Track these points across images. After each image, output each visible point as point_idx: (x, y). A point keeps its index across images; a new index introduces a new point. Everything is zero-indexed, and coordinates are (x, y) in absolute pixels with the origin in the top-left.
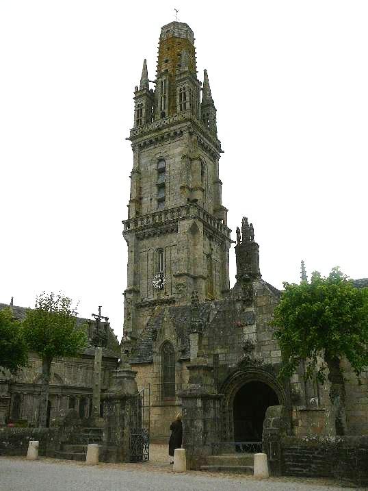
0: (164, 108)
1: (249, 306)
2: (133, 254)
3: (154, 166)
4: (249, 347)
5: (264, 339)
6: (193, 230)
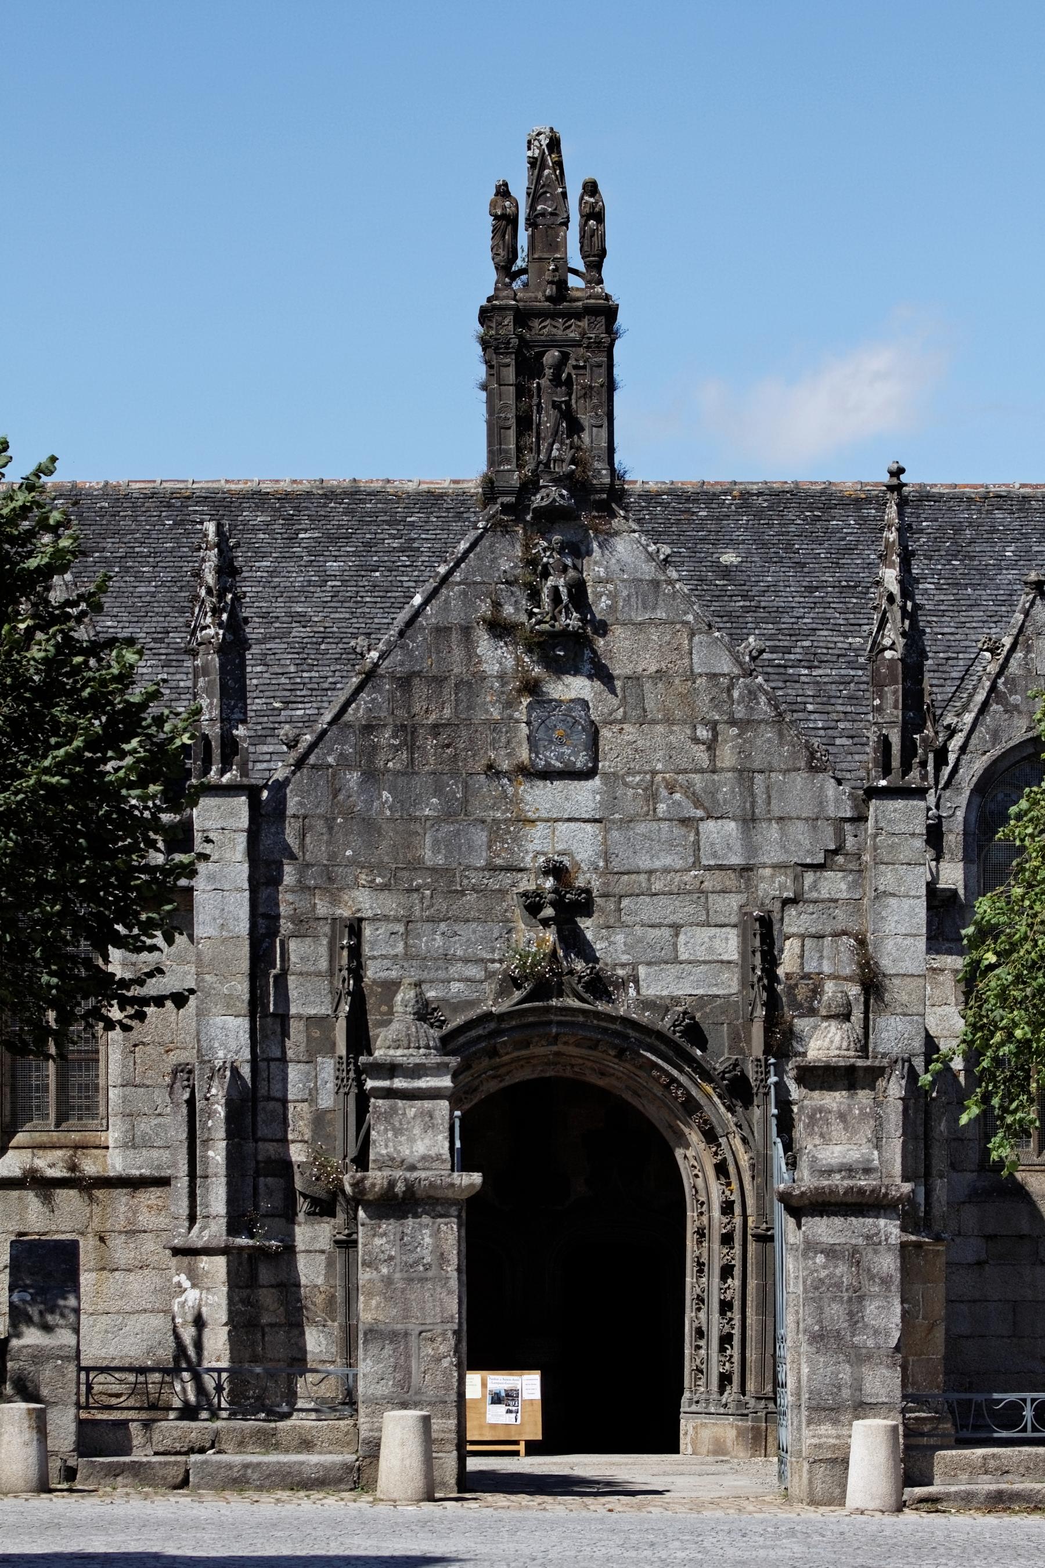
5: (644, 862)
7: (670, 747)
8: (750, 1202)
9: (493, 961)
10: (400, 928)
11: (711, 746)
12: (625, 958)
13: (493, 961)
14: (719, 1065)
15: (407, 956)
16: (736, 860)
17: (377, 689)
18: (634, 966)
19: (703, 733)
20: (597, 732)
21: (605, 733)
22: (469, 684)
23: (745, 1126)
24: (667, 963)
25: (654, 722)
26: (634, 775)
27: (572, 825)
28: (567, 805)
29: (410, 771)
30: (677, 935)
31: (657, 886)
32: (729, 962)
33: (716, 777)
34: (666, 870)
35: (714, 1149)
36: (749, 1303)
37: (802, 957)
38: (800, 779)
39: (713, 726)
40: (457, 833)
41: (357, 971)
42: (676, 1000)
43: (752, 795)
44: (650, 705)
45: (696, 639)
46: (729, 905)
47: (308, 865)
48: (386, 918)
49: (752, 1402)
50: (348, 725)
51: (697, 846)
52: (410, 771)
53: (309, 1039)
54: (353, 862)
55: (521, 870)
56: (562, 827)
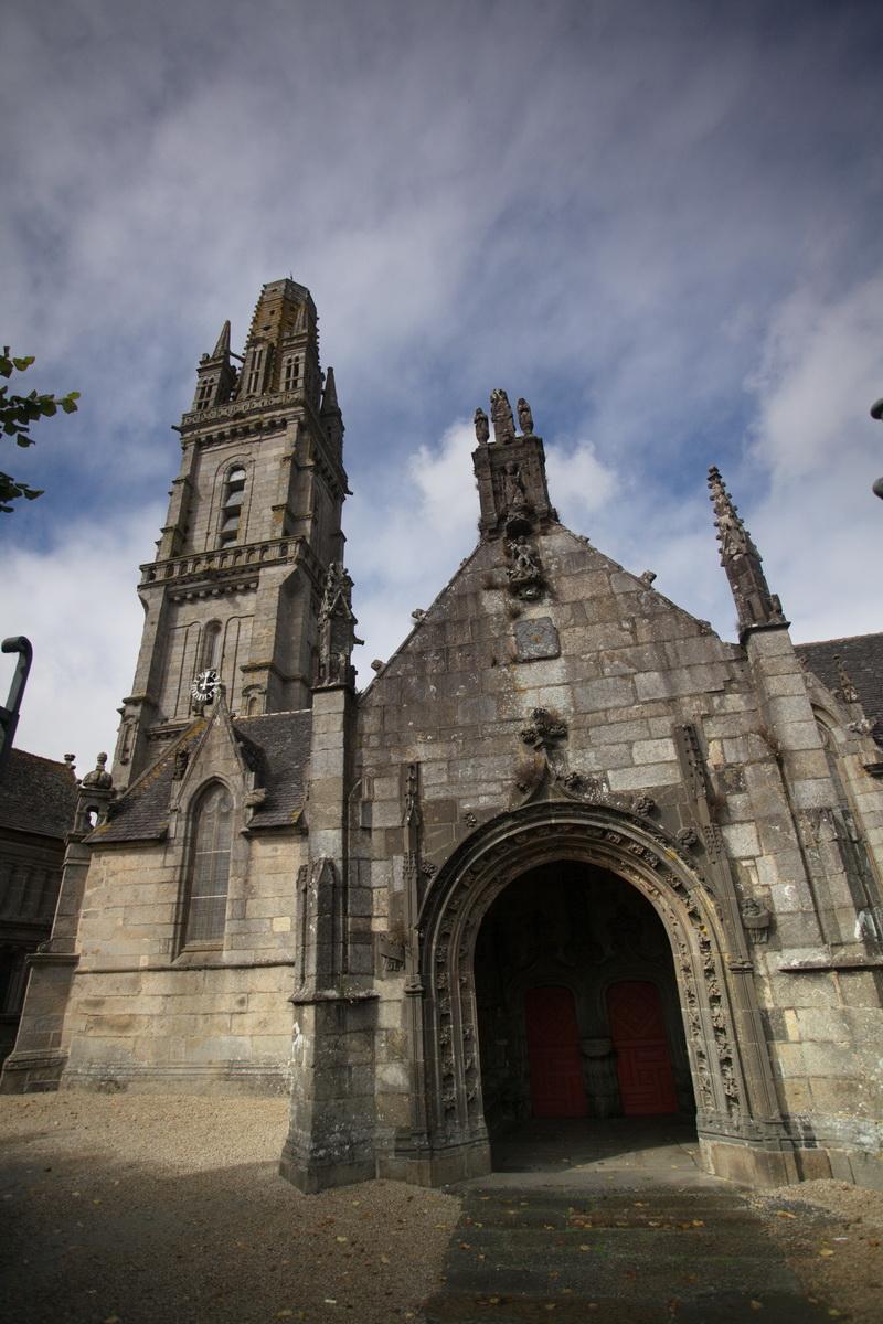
0: (255, 390)
1: (534, 600)
2: (155, 627)
3: (220, 478)
4: (548, 732)
5: (602, 705)
6: (289, 588)
7: (607, 636)
8: (723, 941)
9: (506, 780)
10: (444, 766)
11: (633, 632)
12: (597, 768)
13: (506, 780)
14: (681, 830)
15: (450, 783)
16: (662, 694)
17: (425, 632)
18: (604, 772)
19: (626, 625)
20: (558, 633)
21: (564, 634)
22: (479, 621)
23: (707, 879)
24: (627, 767)
25: (595, 623)
26: (586, 654)
27: (551, 689)
28: (545, 678)
29: (446, 672)
30: (631, 748)
31: (612, 718)
32: (671, 762)
33: (640, 648)
34: (617, 708)
35: (686, 901)
36: (739, 1030)
37: (723, 753)
38: (695, 642)
39: (632, 620)
40: (477, 704)
41: (416, 796)
42: (638, 792)
43: (666, 655)
44: (590, 614)
45: (612, 576)
46: (665, 724)
47: (386, 734)
48: (435, 760)
49: (763, 1128)
50: (409, 653)
51: (634, 690)
52: (446, 672)
53: (387, 844)
54: (415, 728)
55: (520, 720)
56: (543, 691)
